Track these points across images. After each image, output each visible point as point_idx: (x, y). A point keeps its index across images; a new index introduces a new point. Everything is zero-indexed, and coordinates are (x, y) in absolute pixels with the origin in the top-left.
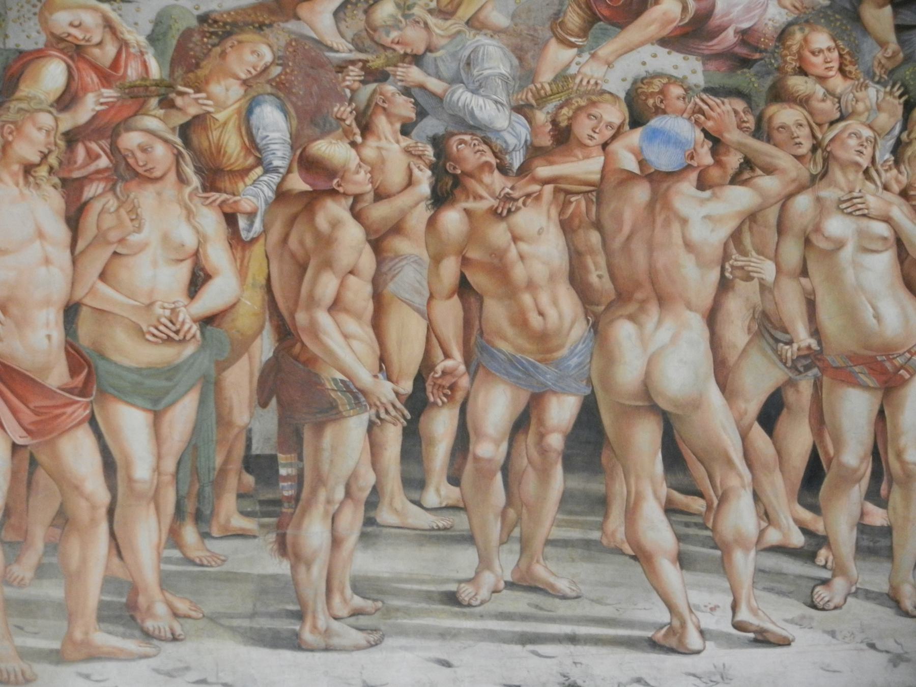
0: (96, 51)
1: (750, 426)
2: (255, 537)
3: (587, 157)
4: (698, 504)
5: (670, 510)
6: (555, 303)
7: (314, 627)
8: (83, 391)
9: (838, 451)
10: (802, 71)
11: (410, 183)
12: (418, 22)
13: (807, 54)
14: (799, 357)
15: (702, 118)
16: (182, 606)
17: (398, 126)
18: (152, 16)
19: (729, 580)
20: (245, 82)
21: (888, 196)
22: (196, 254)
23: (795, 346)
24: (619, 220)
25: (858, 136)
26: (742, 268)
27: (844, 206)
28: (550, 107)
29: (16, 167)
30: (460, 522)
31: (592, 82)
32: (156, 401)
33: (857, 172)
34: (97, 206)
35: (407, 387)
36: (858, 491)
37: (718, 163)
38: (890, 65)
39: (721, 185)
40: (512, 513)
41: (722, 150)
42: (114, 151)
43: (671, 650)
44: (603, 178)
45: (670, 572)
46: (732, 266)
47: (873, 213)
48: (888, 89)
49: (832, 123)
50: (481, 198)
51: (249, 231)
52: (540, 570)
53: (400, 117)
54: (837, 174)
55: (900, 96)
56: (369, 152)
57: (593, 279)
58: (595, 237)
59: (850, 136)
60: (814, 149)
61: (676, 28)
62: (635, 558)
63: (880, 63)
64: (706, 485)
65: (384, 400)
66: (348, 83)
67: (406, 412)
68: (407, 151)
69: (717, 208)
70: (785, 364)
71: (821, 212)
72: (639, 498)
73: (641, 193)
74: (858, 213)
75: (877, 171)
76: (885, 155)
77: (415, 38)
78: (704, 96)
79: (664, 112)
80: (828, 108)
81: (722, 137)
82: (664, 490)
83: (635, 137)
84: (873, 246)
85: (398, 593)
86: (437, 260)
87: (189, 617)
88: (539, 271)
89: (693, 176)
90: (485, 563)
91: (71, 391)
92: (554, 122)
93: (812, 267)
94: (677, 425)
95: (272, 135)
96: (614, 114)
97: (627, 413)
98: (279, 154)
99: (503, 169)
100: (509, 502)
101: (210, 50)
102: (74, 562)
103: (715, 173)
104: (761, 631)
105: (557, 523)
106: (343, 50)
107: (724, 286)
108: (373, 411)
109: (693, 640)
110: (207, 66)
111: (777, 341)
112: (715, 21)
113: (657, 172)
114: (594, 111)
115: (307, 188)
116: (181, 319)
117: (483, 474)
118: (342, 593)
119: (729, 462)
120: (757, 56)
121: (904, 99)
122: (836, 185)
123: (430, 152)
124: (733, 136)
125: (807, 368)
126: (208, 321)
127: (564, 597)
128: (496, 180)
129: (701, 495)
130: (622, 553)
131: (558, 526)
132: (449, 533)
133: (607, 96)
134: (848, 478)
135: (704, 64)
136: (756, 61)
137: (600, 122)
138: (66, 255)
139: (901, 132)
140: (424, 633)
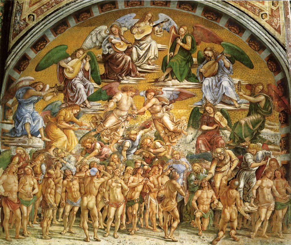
3: (83, 173)
4: (91, 222)
6: (77, 194)
7: (44, 236)
8: (19, 204)
9: (110, 216)
10: (113, 161)
11: (60, 176)
13: (114, 158)
16: (29, 233)
17: (60, 168)
18: (30, 150)
20: (41, 161)
21: (121, 180)
22: (33, 185)
24: (86, 183)
25: (118, 171)
28: (79, 166)
29: (12, 173)
30: (63, 223)
32: (27, 205)
35: (58, 205)
37: (100, 175)
40: (69, 223)
43: (86, 241)
45: (87, 231)
52: (71, 230)
53: (60, 167)
56: (56, 172)
58: (83, 185)
62: (83, 229)
68: (60, 172)
69: (98, 181)
72: (84, 221)
73: (89, 179)
76: (122, 174)
77: (63, 155)
79: (94, 167)
80: (115, 167)
82: (87, 220)
83: (90, 171)
85: (54, 232)
86: (63, 187)
88: (76, 190)
89: (96, 176)
90: (65, 229)
91: (17, 203)
92: (79, 168)
93: (110, 191)
96: (87, 167)
97: (85, 209)
99: (72, 175)
100: (68, 221)
102: (17, 226)
103: (99, 176)
104: (97, 239)
105: (74, 224)
106: (54, 156)
107: (99, 192)
109: (89, 240)
112: (102, 153)
113: (92, 176)
114: (85, 167)
118: (48, 232)
119: (96, 217)
120: (107, 159)
122: (115, 178)
123: (63, 172)
124: (102, 171)
125: (107, 204)
126: (34, 195)
127: (74, 234)
128: (71, 176)
129: (92, 221)
130: (81, 228)
138: (18, 185)
140: (57, 237)
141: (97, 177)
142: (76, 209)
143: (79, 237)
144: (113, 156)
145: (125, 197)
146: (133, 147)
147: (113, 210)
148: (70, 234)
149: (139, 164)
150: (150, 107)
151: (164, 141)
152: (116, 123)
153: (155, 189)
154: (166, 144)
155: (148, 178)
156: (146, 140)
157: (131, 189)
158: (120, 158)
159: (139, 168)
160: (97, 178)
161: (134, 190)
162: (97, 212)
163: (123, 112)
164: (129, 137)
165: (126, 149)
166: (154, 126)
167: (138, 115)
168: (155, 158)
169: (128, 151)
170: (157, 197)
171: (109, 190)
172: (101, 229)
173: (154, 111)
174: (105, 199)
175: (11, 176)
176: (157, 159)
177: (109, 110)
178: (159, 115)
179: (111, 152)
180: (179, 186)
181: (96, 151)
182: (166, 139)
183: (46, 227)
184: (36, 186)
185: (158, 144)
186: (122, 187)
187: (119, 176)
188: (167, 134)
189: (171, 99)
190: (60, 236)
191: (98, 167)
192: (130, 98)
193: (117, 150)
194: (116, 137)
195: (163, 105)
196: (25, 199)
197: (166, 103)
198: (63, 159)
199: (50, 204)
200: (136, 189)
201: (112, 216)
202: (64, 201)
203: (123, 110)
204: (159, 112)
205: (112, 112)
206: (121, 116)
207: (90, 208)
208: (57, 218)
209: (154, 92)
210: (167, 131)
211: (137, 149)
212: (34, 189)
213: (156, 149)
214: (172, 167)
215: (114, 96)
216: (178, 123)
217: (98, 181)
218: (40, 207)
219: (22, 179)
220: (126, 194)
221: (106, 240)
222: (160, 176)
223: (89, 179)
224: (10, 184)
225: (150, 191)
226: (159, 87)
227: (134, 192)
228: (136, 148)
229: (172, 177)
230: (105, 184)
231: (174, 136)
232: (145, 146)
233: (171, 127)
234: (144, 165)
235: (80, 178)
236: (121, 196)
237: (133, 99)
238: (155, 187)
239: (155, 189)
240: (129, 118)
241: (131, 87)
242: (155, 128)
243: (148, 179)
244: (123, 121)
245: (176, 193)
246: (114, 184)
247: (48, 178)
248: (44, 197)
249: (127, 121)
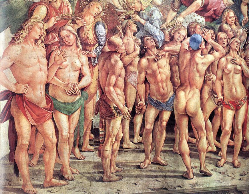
0: (55, 4)
1: (207, 120)
2: (93, 152)
4: (194, 141)
5: (189, 142)
6: (167, 86)
7: (107, 175)
8: (50, 110)
10: (226, 23)
11: (135, 51)
12: (139, 1)
14: (219, 102)
16: (75, 171)
17: (132, 33)
19: (200, 160)
20: (94, 17)
22: (80, 69)
23: (218, 98)
25: (237, 42)
26: (208, 77)
27: (232, 61)
28: (169, 29)
29: (32, 40)
30: (142, 147)
31: (180, 23)
33: (236, 52)
34: (54, 54)
35: (131, 109)
36: (228, 137)
37: (206, 48)
39: (206, 54)
42: (59, 36)
44: (180, 51)
46: (206, 76)
47: (238, 63)
48: (244, 29)
50: (152, 55)
51: (94, 63)
52: (159, 158)
53: (134, 30)
54: (231, 52)
55: (247, 32)
56: (125, 40)
57: (176, 79)
58: (177, 67)
59: (235, 42)
60: (227, 45)
61: (200, 8)
62: (180, 155)
63: (243, 22)
64: (196, 135)
65: (126, 113)
66: (121, 19)
67: (131, 116)
68: (134, 41)
70: (216, 103)
71: (227, 63)
72: (182, 139)
74: (235, 63)
75: (240, 52)
78: (205, 29)
81: (208, 40)
82: (188, 137)
84: (237, 73)
85: (127, 166)
86: (140, 73)
87: (76, 174)
89: (200, 51)
91: (46, 109)
92: (170, 34)
93: (224, 79)
94: (191, 119)
95: (101, 34)
96: (184, 33)
98: (103, 40)
99: (157, 47)
100: (153, 141)
101: (85, 6)
103: (205, 51)
105: (164, 146)
107: (205, 82)
108: (123, 116)
110: (85, 10)
111: (214, 97)
112: (208, 7)
114: (180, 31)
115: (109, 51)
116: (76, 88)
117: (147, 134)
118: (114, 166)
119: (202, 130)
120: (217, 18)
123: (140, 41)
124: (210, 40)
125: (220, 105)
126: (82, 89)
127: (164, 165)
128: (155, 50)
129: (195, 138)
131: (164, 147)
132: (139, 150)
133: (183, 27)
134: (226, 134)
135: (205, 19)
136: (217, 19)
137: (181, 35)
139: (246, 42)
141: (202, 52)
142: (166, 116)
143: (174, 172)
144: (227, 13)
147: (229, 114)
148: (158, 166)
162: (203, 120)
171: (222, 76)
172: (211, 152)
174: (215, 96)
175: (30, 46)
183: (110, 156)
184: (86, 70)
186: (242, 71)
190: (137, 172)
191: (204, 33)
196: (63, 98)
198: (139, 15)
199: (117, 108)
201: (228, 128)
202: (143, 100)
207: (191, 113)
208: (132, 136)
212: (81, 77)
217: (204, 61)
218: (96, 114)
219: (56, 54)
221: (220, 173)
223: (188, 56)
224: (29, 66)
230: (215, 66)
235: (171, 54)
246: (230, 66)
247: (111, 53)
248: (103, 93)
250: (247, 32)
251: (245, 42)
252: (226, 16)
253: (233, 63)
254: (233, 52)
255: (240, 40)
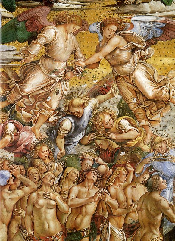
10: (39, 158)
15: (12, 171)
23: (28, 234)
25: (50, 176)
27: (44, 196)
33: (49, 187)
38: (61, 156)
39: (15, 190)
41: (16, 180)
47: (52, 198)
49: (44, 173)
54: (44, 187)
55: (63, 165)
69: (12, 196)
74: (48, 198)
75: (54, 186)
76: (56, 181)
81: (16, 176)
84: (51, 208)
89: (8, 187)
103: (14, 186)
107: (13, 217)
111: (23, 232)
112: (19, 143)
120: (28, 153)
121: (64, 166)
124: (19, 176)
139: (61, 176)
141: (10, 187)
144: (39, 147)
145: (64, 226)
146: (77, 129)
149: (90, 163)
150: (110, 54)
151: (135, 117)
152: (44, 85)
153: (120, 210)
154: (141, 124)
155: (107, 188)
156: (101, 117)
157: (74, 210)
158: (53, 152)
159: (89, 171)
160: (10, 190)
161: (81, 213)
163: (57, 64)
164: (69, 111)
165: (64, 133)
166: (117, 89)
167: (87, 70)
168: (119, 151)
169: (68, 138)
170: (125, 225)
173: (116, 60)
174: (24, 231)
176: (123, 153)
177: (32, 60)
178: (126, 68)
179: (35, 140)
180: (165, 203)
181: (8, 138)
182: (140, 113)
185: (125, 123)
186: (57, 206)
187: (51, 187)
188: (141, 104)
189: (149, 38)
191: (12, 169)
192: (70, 36)
193: (47, 137)
194: (44, 112)
195: (134, 50)
197: (139, 46)
200: (84, 209)
203: (58, 58)
204: (126, 63)
205: (36, 63)
206: (54, 72)
209: (116, 24)
210: (142, 100)
211: (85, 135)
213: (121, 133)
214: (151, 167)
215: (40, 33)
216: (162, 83)
217: (12, 196)
220: (64, 220)
222: (129, 185)
225: (111, 214)
226: (126, 16)
227: (81, 216)
228: (84, 133)
229: (152, 187)
231: (155, 108)
232: (99, 127)
233: (150, 90)
234: (100, 165)
236: (55, 224)
237: (76, 38)
238: (119, 207)
239: (120, 210)
240: (69, 74)
241: (73, 16)
242: (118, 92)
243: (106, 191)
244: (58, 81)
245: (160, 217)
246: (41, 201)
249: (66, 80)
250: (63, 165)
251: (60, 176)
252: (38, 151)
253: (46, 198)
254: (46, 187)
255: (54, 174)
